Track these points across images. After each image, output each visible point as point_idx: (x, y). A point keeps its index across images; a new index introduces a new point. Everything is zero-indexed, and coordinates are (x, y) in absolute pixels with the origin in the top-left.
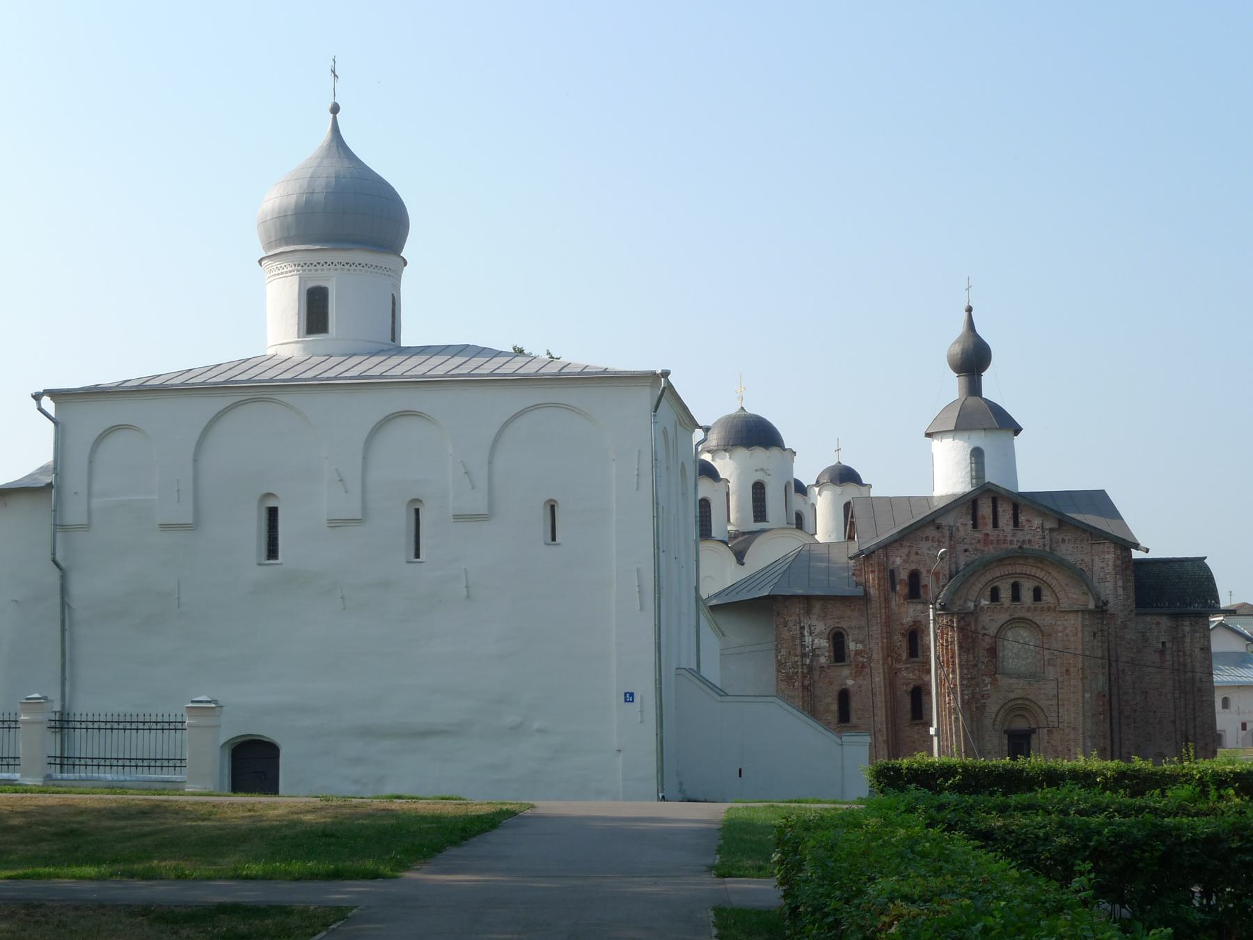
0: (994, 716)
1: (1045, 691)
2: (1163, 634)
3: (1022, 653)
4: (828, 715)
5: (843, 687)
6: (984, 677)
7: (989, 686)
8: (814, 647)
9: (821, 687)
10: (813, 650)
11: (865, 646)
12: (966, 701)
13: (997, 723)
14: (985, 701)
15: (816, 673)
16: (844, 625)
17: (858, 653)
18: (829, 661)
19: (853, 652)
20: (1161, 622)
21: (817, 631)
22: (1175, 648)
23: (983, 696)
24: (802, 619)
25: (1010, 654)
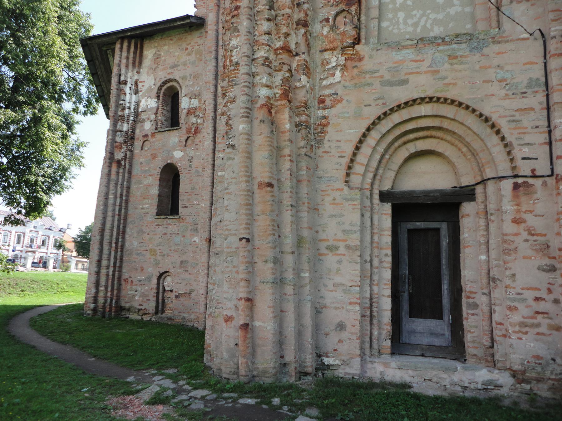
0: (349, 149)
1: (501, 74)
4: (146, 201)
5: (169, 162)
6: (327, 55)
7: (338, 74)
8: (140, 110)
9: (141, 163)
10: (137, 114)
11: (200, 100)
12: (261, 101)
13: (358, 169)
14: (326, 112)
15: (138, 144)
16: (177, 75)
17: (190, 112)
18: (154, 127)
19: (185, 111)
21: (144, 89)
23: (322, 101)
24: (123, 71)
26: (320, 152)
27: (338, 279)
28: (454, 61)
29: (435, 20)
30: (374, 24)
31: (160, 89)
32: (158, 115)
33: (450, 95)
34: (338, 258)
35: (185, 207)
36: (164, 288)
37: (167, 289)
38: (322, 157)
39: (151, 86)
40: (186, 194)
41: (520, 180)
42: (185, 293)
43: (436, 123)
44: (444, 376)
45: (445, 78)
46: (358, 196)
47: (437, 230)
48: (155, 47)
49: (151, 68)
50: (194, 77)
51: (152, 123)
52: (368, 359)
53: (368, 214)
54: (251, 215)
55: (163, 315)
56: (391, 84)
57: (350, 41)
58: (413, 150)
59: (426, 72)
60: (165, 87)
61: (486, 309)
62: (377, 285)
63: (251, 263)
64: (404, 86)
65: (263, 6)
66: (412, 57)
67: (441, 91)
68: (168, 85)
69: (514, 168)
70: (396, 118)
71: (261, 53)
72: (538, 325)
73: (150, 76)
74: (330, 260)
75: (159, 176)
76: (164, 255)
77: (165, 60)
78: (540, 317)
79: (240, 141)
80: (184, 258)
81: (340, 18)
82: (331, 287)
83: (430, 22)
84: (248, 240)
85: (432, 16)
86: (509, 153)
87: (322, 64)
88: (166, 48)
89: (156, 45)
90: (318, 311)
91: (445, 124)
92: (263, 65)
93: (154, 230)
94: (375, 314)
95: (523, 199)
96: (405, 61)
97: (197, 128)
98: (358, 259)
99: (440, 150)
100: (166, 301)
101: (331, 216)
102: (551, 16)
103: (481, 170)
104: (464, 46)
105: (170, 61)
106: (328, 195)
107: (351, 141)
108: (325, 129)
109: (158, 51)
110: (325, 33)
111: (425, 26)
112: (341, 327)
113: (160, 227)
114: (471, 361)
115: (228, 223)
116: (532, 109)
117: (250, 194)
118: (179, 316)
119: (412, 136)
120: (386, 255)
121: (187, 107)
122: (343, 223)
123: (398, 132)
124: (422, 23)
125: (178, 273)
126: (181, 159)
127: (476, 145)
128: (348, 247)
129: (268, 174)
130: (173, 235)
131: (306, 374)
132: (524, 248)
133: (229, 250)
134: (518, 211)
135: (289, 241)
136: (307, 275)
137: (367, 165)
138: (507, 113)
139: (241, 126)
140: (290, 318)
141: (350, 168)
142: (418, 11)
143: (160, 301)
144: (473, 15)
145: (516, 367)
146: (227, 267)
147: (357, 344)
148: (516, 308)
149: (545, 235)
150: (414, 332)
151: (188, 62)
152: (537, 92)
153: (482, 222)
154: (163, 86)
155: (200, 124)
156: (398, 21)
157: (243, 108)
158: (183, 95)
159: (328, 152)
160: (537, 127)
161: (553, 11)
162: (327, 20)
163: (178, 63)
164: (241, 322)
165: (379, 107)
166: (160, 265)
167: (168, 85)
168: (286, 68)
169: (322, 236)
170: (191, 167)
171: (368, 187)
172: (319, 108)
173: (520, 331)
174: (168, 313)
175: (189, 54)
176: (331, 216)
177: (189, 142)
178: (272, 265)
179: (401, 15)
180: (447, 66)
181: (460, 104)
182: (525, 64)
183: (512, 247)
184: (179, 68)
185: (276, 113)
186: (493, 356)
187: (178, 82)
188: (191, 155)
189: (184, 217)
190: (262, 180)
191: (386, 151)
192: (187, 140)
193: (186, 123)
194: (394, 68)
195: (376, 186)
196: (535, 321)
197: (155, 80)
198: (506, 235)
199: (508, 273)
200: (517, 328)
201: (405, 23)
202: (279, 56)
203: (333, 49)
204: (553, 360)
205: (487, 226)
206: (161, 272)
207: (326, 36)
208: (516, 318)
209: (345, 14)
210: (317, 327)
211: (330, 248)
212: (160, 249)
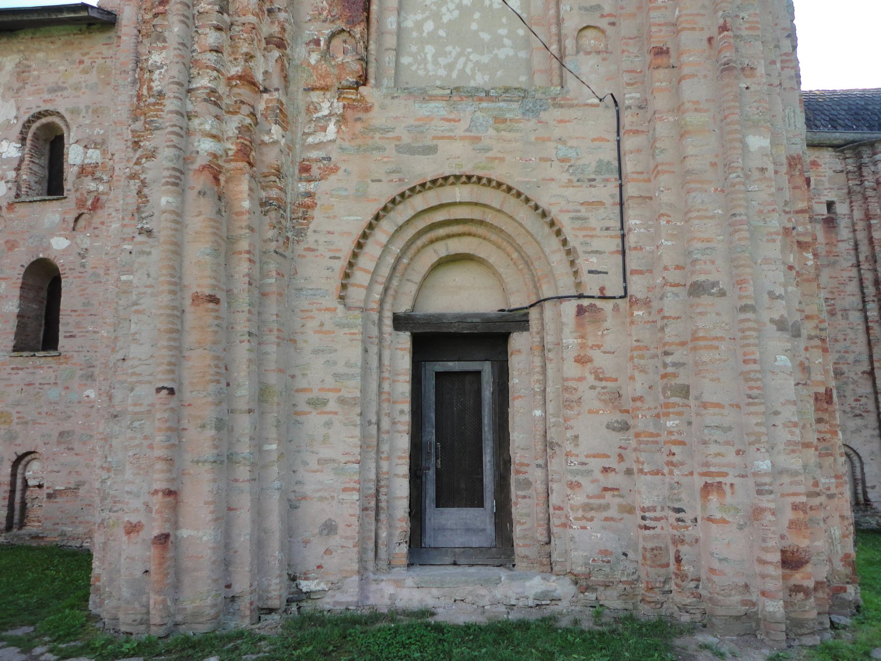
0: (347, 246)
1: (563, 151)
2: (827, 185)
3: (474, 26)
5: (41, 256)
6: (315, 96)
7: (332, 128)
11: (104, 153)
13: (361, 277)
14: (311, 187)
16: (61, 105)
17: (83, 171)
18: (13, 193)
19: (75, 170)
20: (820, 161)
22: (858, 214)
23: (305, 169)
25: (429, 26)
26: (300, 249)
27: (325, 452)
28: (502, 126)
29: (477, 63)
30: (389, 58)
31: (27, 125)
32: (21, 172)
33: (496, 174)
34: (324, 418)
35: (71, 336)
36: (25, 481)
37: (31, 483)
38: (304, 256)
39: (9, 121)
40: (74, 314)
41: (586, 302)
42: (67, 489)
43: (475, 214)
44: (483, 591)
45: (489, 149)
46: (359, 321)
47: (478, 374)
48: (19, 51)
49: (10, 88)
50: (95, 111)
51: (10, 185)
52: (372, 576)
53: (374, 349)
54: (179, 349)
55: (23, 531)
56: (411, 150)
57: (352, 79)
58: (443, 253)
59: (462, 138)
60: (38, 124)
61: (540, 487)
62: (388, 459)
63: (176, 431)
64: (430, 156)
65: (209, 4)
66: (443, 113)
67: (484, 168)
68: (44, 120)
69: (578, 285)
70: (419, 202)
71: (203, 82)
72: (606, 507)
73: (7, 101)
74: (314, 421)
75: (20, 281)
76: (26, 423)
77: (39, 77)
78: (608, 495)
79: (162, 225)
80: (67, 426)
81: (337, 42)
82: (314, 465)
83: (470, 65)
84: (171, 391)
85: (474, 57)
86: (572, 263)
87: (308, 109)
88: (41, 55)
89: (22, 48)
90: (292, 505)
91: (489, 217)
92: (205, 100)
93: (7, 377)
94: (383, 504)
95: (589, 328)
96: (432, 119)
97: (97, 200)
98: (358, 420)
99: (482, 255)
100: (29, 505)
101: (316, 352)
102: (626, 78)
103: (537, 288)
104: (515, 106)
105: (49, 79)
106: (312, 317)
107: (349, 234)
108: (310, 212)
109: (26, 59)
110: (313, 61)
111: (463, 70)
112: (329, 528)
113: (20, 372)
114: (521, 565)
115: (136, 362)
116: (601, 203)
117: (177, 313)
118: (55, 530)
119: (442, 232)
120: (402, 412)
121: (78, 161)
122: (335, 363)
123: (421, 224)
124: (460, 65)
125: (54, 454)
126: (66, 252)
127: (530, 250)
128: (342, 401)
129: (210, 281)
130: (46, 387)
131: (270, 611)
132: (591, 400)
133: (137, 409)
134: (583, 346)
135: (244, 392)
136: (274, 446)
137: (374, 273)
138: (571, 207)
139: (164, 200)
140: (244, 518)
141: (347, 276)
142: (454, 48)
143: (17, 506)
144: (529, 62)
145: (579, 569)
146: (133, 438)
147: (354, 554)
148: (579, 485)
149: (616, 380)
150: (442, 529)
151: (83, 85)
152: (608, 180)
153: (538, 362)
154: (34, 122)
155: (103, 193)
156: (425, 58)
157: (168, 169)
158: (71, 141)
159: (314, 250)
160: (607, 229)
161: (627, 71)
162: (317, 42)
163: (65, 85)
164: (156, 532)
165: (393, 184)
166: (18, 441)
167: (44, 120)
168: (246, 110)
169: (302, 383)
170: (83, 266)
171: (375, 306)
172: (300, 180)
173: (584, 518)
174: (32, 528)
175: (85, 72)
176: (316, 352)
177: (82, 222)
178: (213, 432)
179: (430, 50)
180: (491, 132)
181: (509, 189)
182: (593, 140)
183: (575, 397)
184: (65, 93)
185: (226, 182)
186: (550, 556)
187: (62, 117)
188: (85, 246)
189: (69, 354)
190: (198, 290)
191: (404, 251)
192: (77, 220)
193: (77, 190)
194: (416, 127)
195: (387, 306)
196: (602, 501)
197: (18, 109)
198: (566, 379)
199: (569, 433)
200: (580, 514)
201: (436, 63)
202: (235, 90)
203: (325, 89)
204: (625, 554)
205: (544, 368)
206: (20, 453)
207: (315, 67)
208: (579, 498)
209: (345, 36)
210: (290, 532)
211: (311, 403)
212: (18, 412)
